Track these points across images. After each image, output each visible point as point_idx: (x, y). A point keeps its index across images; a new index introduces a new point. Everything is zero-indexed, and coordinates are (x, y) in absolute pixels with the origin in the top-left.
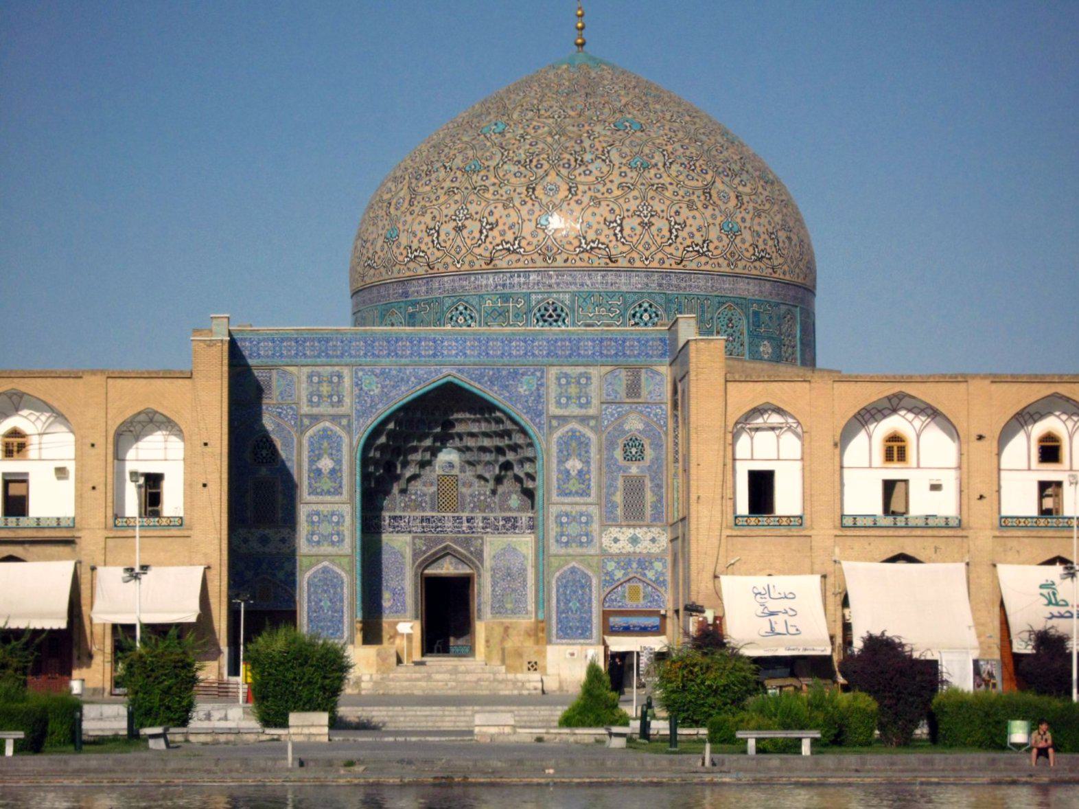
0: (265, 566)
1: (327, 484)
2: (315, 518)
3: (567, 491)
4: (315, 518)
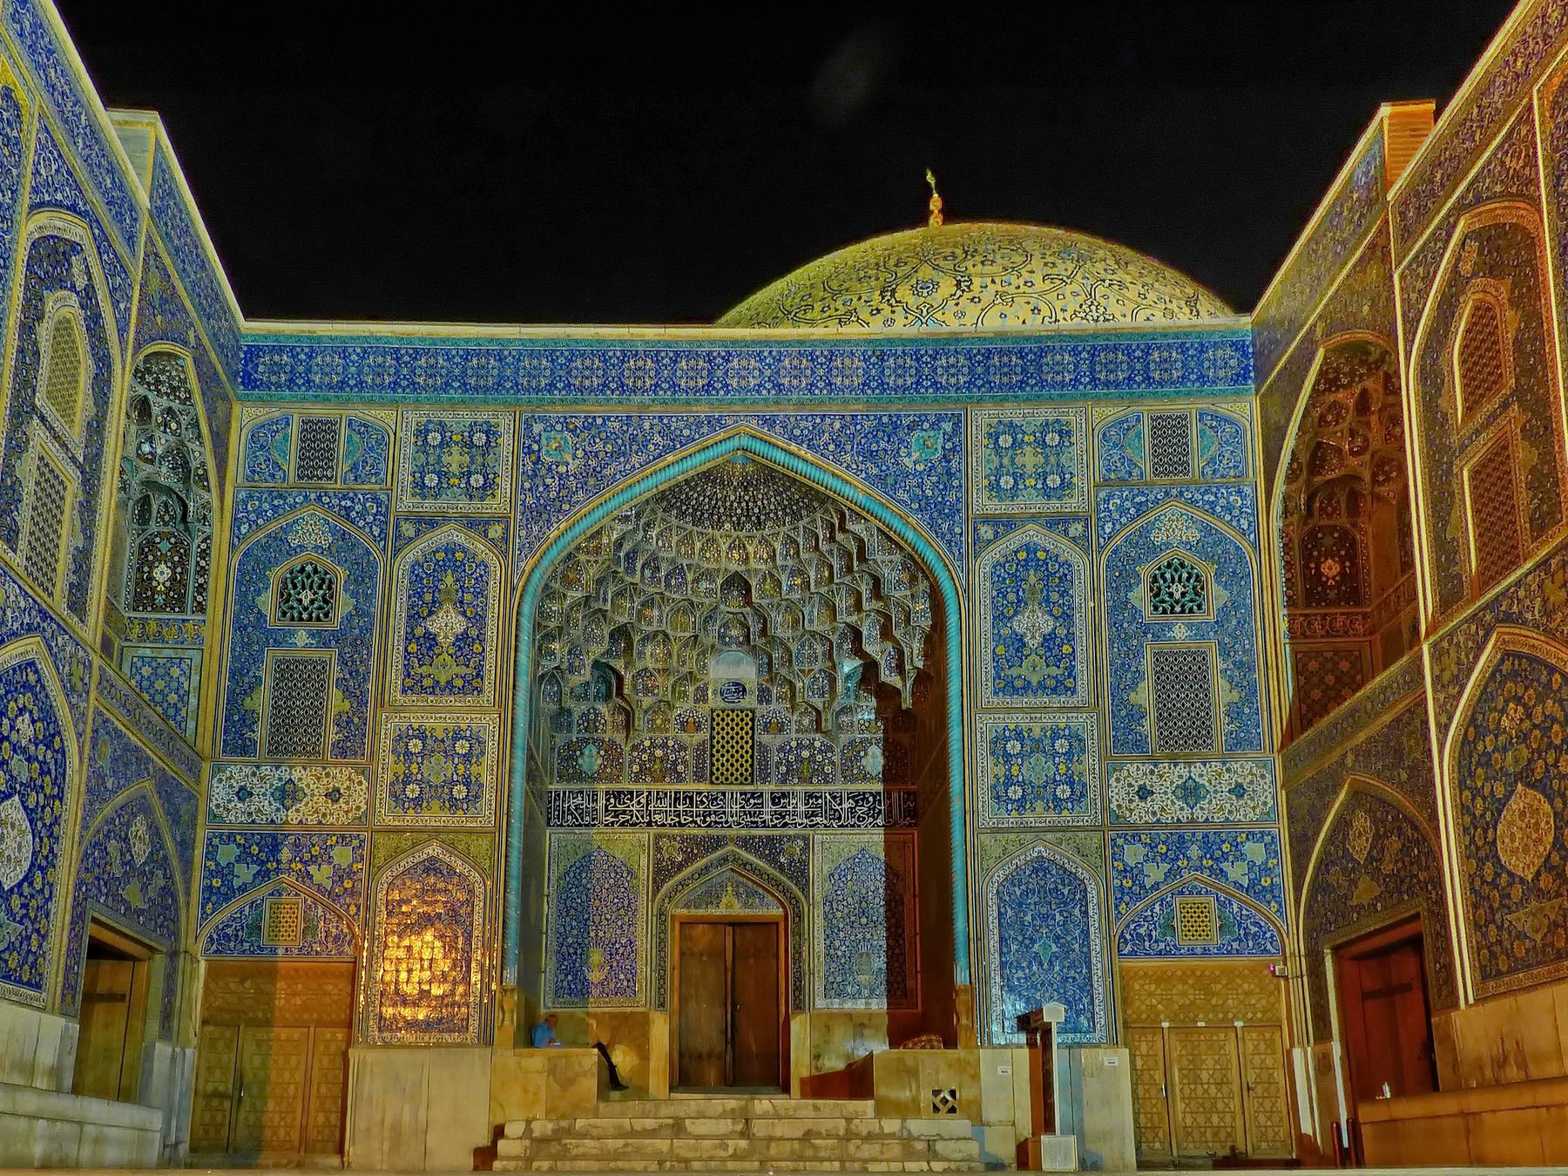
0: (285, 854)
1: (446, 668)
2: (415, 746)
3: (1018, 683)
4: (415, 746)
